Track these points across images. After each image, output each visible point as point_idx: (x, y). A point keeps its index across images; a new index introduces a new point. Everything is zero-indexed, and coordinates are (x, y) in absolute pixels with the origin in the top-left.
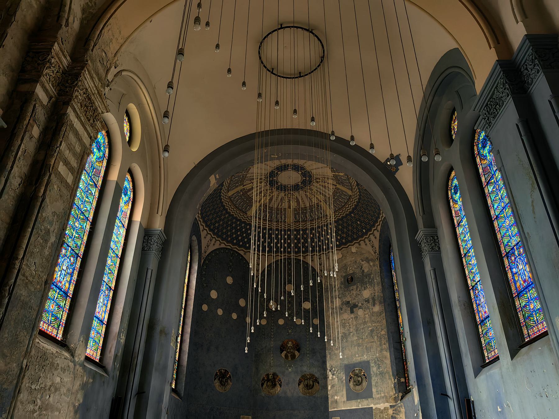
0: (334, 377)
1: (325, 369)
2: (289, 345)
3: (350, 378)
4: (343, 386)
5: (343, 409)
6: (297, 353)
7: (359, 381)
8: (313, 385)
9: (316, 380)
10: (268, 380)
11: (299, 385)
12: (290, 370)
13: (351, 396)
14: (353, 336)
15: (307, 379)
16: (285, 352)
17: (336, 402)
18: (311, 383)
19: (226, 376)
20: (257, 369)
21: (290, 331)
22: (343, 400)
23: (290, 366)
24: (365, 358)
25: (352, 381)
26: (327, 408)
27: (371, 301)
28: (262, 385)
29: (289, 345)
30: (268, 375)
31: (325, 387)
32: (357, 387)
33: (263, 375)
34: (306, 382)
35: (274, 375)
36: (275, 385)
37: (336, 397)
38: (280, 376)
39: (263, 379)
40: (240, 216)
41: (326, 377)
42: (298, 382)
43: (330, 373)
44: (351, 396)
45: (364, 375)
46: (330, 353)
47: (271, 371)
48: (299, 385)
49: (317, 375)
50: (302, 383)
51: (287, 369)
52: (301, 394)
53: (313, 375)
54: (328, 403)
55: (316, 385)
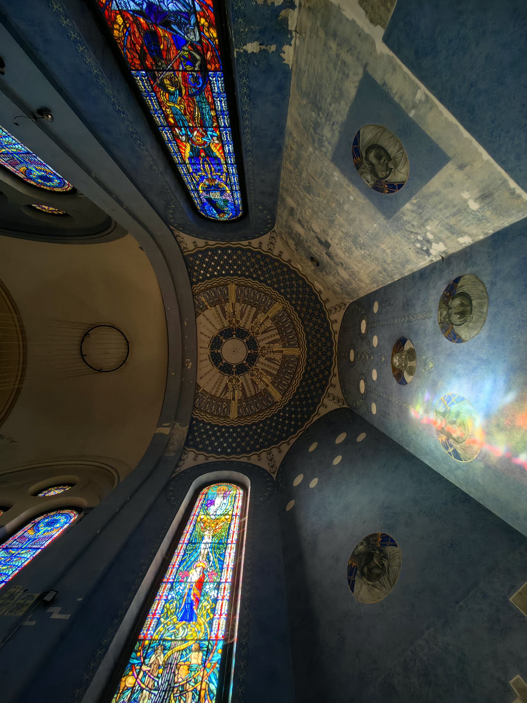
7: (378, 157)
12: (431, 365)
40: (275, 410)
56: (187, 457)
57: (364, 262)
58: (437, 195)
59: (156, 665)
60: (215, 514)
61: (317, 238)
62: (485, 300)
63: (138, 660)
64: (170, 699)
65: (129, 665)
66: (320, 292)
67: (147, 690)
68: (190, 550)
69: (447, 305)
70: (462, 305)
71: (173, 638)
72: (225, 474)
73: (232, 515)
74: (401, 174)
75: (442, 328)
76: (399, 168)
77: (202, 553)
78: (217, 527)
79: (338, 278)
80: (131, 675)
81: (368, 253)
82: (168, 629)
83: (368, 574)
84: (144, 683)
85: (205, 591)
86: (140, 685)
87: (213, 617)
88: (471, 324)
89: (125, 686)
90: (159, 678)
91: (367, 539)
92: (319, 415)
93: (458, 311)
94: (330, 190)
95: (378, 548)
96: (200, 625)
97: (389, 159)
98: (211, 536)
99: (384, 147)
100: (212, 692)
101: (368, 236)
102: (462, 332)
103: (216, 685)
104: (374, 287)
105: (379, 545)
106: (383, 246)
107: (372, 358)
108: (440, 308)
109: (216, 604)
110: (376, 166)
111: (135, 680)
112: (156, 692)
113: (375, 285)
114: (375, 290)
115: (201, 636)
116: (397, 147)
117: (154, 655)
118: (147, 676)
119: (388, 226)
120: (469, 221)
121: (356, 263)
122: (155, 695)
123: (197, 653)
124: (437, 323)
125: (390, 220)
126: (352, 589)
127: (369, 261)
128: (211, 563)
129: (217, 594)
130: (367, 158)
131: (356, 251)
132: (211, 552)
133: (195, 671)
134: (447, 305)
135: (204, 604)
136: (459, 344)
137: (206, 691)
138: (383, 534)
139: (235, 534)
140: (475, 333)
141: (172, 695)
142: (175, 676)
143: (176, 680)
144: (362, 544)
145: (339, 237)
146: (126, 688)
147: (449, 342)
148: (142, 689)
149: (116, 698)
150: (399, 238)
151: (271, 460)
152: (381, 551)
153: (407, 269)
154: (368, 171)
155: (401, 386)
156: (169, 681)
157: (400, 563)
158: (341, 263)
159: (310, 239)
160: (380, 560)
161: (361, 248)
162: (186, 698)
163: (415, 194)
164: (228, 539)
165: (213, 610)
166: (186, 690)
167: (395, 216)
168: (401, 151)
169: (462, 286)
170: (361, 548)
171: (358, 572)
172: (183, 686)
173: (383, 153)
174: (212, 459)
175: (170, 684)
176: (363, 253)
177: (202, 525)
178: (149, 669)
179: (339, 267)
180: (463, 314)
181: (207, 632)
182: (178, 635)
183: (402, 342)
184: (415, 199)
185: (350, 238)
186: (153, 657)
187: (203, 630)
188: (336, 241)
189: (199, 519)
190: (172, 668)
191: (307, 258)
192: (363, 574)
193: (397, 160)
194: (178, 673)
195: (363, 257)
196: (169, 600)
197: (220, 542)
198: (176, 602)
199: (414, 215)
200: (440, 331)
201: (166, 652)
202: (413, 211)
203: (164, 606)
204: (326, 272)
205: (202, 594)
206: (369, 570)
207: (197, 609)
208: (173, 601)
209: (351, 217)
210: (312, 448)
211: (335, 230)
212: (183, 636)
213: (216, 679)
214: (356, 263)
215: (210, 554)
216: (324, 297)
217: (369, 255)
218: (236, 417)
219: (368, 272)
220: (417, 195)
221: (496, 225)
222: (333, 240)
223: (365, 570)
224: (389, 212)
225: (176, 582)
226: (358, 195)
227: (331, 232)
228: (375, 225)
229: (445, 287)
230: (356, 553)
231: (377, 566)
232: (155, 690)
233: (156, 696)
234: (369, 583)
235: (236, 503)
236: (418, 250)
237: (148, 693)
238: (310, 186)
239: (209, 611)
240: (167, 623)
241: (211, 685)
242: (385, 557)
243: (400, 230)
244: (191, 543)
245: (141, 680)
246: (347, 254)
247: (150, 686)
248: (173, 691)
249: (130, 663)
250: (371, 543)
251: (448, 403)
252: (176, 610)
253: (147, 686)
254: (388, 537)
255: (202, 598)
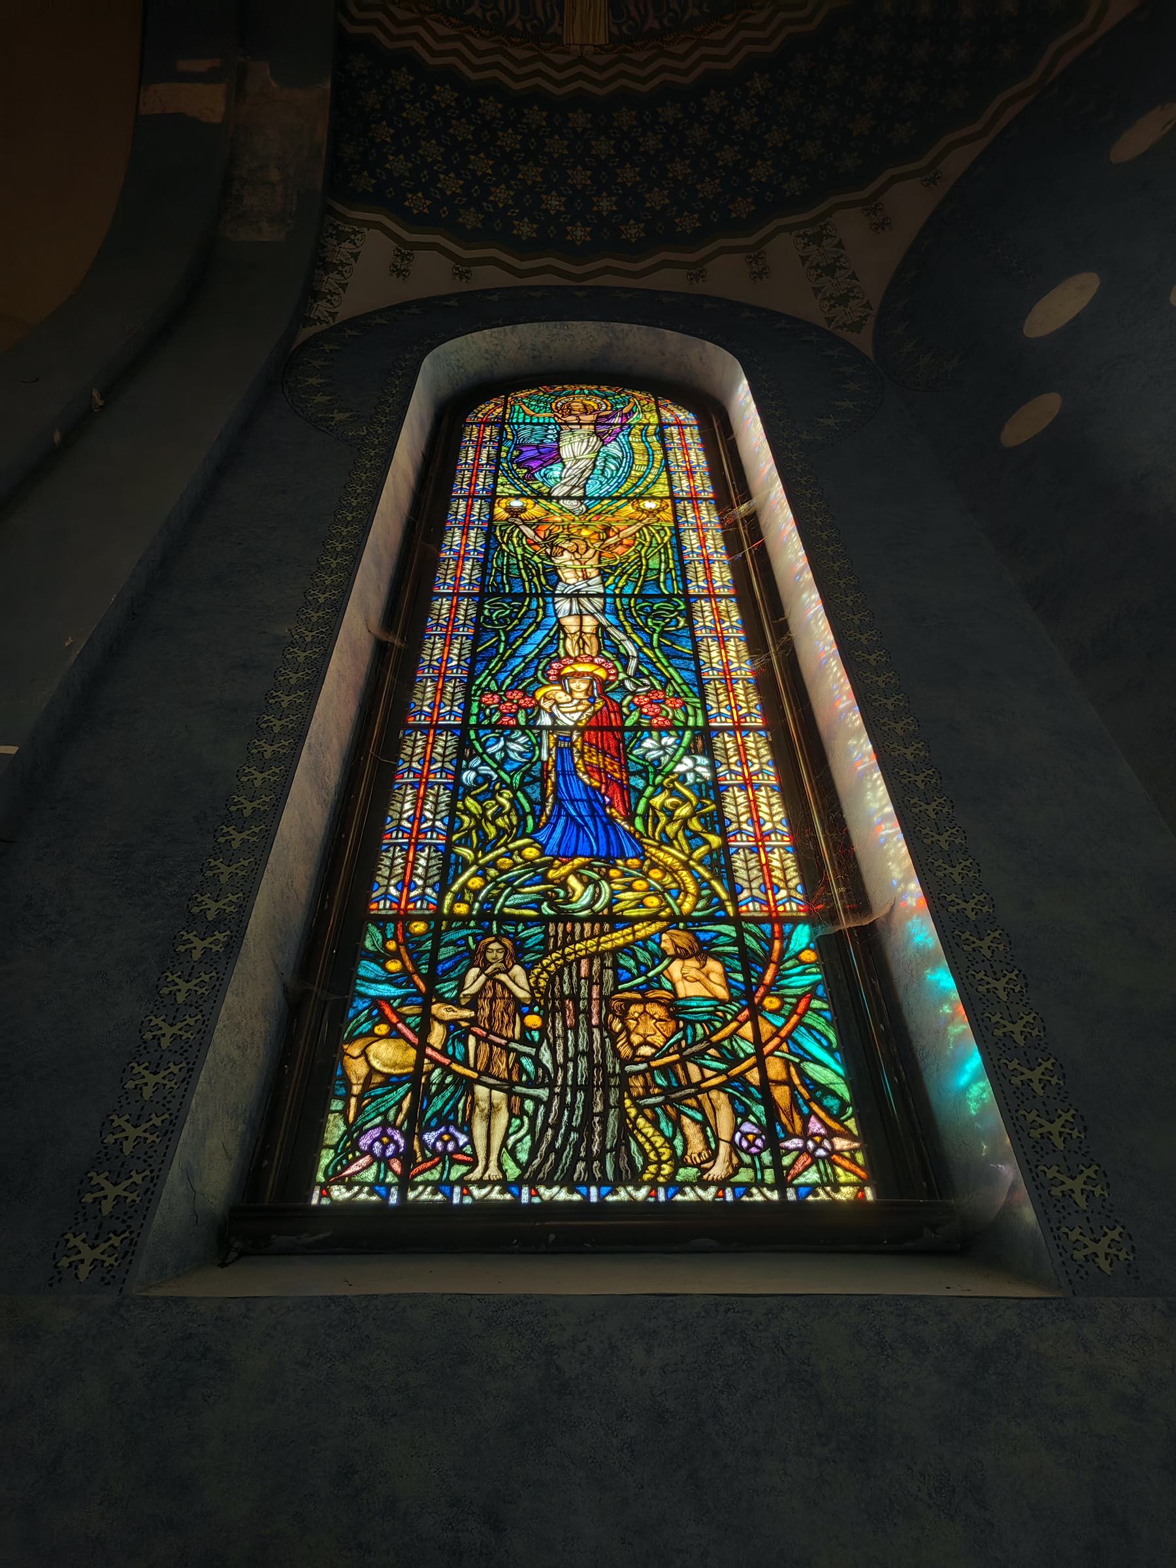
56: (355, 256)
59: (500, 1004)
60: (578, 493)
63: (398, 986)
64: (623, 1114)
65: (360, 1004)
67: (491, 1087)
68: (502, 620)
71: (546, 909)
72: (582, 337)
73: (673, 498)
77: (571, 624)
78: (611, 541)
80: (387, 1036)
82: (509, 883)
84: (465, 1063)
85: (643, 757)
86: (447, 1070)
87: (725, 847)
89: (372, 1070)
90: (537, 1046)
96: (667, 870)
98: (594, 573)
100: (828, 1091)
103: (840, 1071)
109: (719, 801)
111: (413, 1053)
112: (543, 1093)
115: (687, 907)
117: (474, 971)
118: (472, 1041)
122: (537, 1101)
123: (692, 963)
128: (633, 663)
129: (713, 767)
132: (621, 627)
133: (708, 1022)
135: (657, 801)
137: (793, 1087)
139: (715, 567)
141: (628, 1103)
142: (614, 1037)
143: (626, 1051)
146: (377, 1079)
148: (466, 1086)
149: (344, 1112)
151: (830, 270)
156: (589, 1054)
162: (700, 1109)
164: (685, 582)
165: (717, 822)
166: (690, 1085)
172: (665, 1070)
174: (488, 278)
175: (604, 1066)
177: (529, 532)
178: (467, 1013)
181: (715, 894)
182: (567, 900)
186: (474, 980)
187: (692, 888)
189: (500, 512)
190: (588, 1013)
194: (625, 1028)
196: (468, 791)
197: (651, 591)
198: (507, 793)
201: (528, 958)
203: (452, 806)
205: (633, 768)
207: (630, 820)
208: (493, 794)
212: (597, 907)
213: (829, 1049)
215: (618, 635)
218: (602, 40)
225: (478, 726)
232: (531, 1084)
233: (548, 1105)
235: (676, 456)
237: (498, 1096)
239: (695, 825)
240: (493, 864)
241: (811, 1068)
244: (498, 593)
245: (443, 1051)
247: (500, 1067)
248: (625, 1087)
249: (363, 996)
252: (522, 818)
253: (487, 1072)
255: (639, 782)
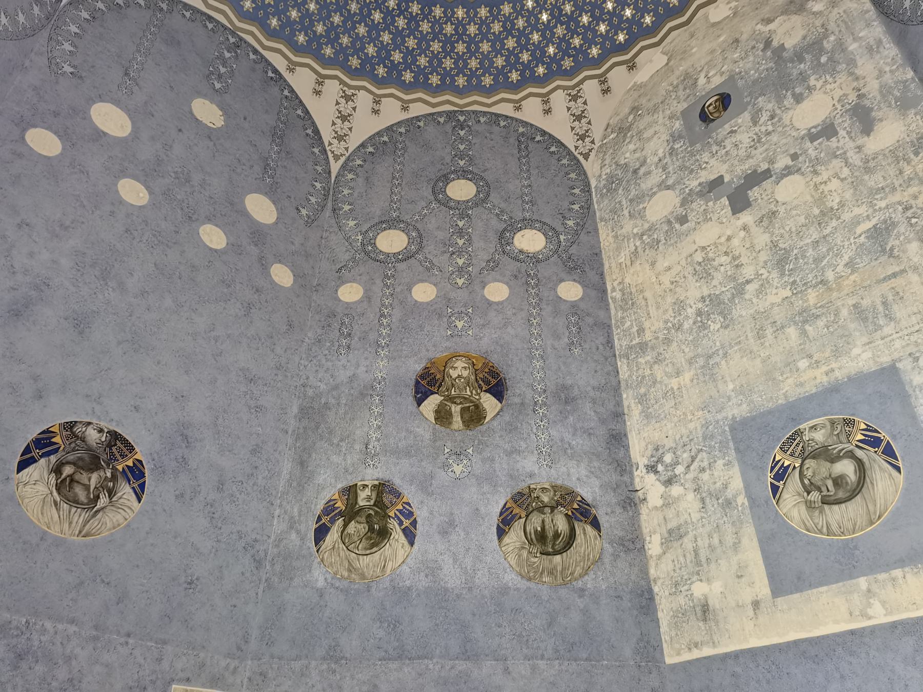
0: (676, 490)
1: (624, 467)
2: (454, 374)
3: (779, 477)
4: (737, 524)
5: (755, 642)
6: (489, 402)
7: (839, 481)
8: (572, 530)
9: (583, 513)
10: (351, 513)
11: (501, 533)
12: (458, 469)
13: (788, 576)
14: (760, 292)
15: (540, 510)
16: (434, 401)
17: (705, 610)
18: (562, 525)
19: (112, 459)
20: (302, 464)
21: (460, 324)
22: (747, 596)
23: (458, 455)
24: (861, 358)
25: (793, 484)
26: (649, 648)
27: (844, 124)
28: (321, 533)
29: (454, 374)
30: (351, 492)
31: (632, 543)
32: (835, 514)
33: (327, 488)
34: (535, 522)
35: (382, 488)
36: (384, 534)
37: (699, 589)
38: (410, 494)
39: (329, 509)
41: (631, 501)
42: (494, 520)
43: (652, 477)
44: (788, 576)
45: (874, 442)
46: (642, 399)
47: (371, 475)
48: (501, 533)
49: (586, 492)
50: (518, 525)
51: (445, 466)
52: (511, 578)
53: (571, 493)
54: (656, 621)
55: (584, 532)
57: (670, 300)
58: (735, 544)
61: (767, 174)
62: (560, 581)
66: (631, 66)
69: (558, 504)
70: (557, 535)
74: (792, 505)
75: (520, 494)
76: (803, 508)
79: (656, 177)
81: (686, 326)
83: (65, 479)
88: (525, 553)
91: (115, 437)
92: (291, 70)
93: (547, 527)
94: (844, 312)
95: (114, 468)
97: (826, 501)
99: (848, 503)
101: (716, 353)
102: (515, 537)
104: (614, 290)
105: (120, 468)
106: (687, 376)
107: (460, 282)
108: (555, 488)
110: (829, 464)
113: (618, 295)
114: (609, 288)
116: (834, 527)
119: (719, 417)
120: (680, 569)
121: (674, 272)
124: (529, 481)
125: (727, 428)
126: (23, 465)
127: (667, 316)
130: (851, 455)
131: (699, 296)
134: (558, 504)
136: (495, 531)
138: (140, 462)
140: (513, 563)
144: (101, 431)
145: (744, 260)
147: (499, 510)
150: (691, 426)
152: (114, 478)
153: (633, 405)
154: (830, 442)
155: (410, 392)
157: (119, 525)
158: (683, 220)
159: (774, 138)
160: (101, 486)
161: (699, 313)
163: (751, 508)
167: (731, 444)
168: (825, 530)
169: (585, 534)
170: (92, 436)
171: (53, 458)
173: (841, 494)
176: (689, 310)
179: (677, 201)
180: (541, 537)
183: (497, 385)
184: (743, 504)
185: (729, 295)
188: (736, 242)
191: (731, 79)
192: (57, 470)
193: (817, 513)
195: (680, 306)
199: (718, 485)
200: (515, 491)
202: (726, 486)
204: (680, 137)
206: (72, 479)
209: (769, 331)
210: (207, 112)
211: (763, 257)
214: (674, 272)
216: (618, 77)
217: (681, 325)
219: (648, 294)
220: (748, 511)
221: (663, 601)
222: (742, 234)
223: (68, 470)
224: (744, 435)
226: (801, 385)
227: (762, 239)
228: (731, 386)
229: (589, 498)
230: (78, 429)
231: (87, 488)
234: (55, 494)
236: (661, 451)
238: (884, 251)
242: (111, 493)
243: (705, 438)
246: (699, 257)
250: (114, 449)
251: (400, 511)
254: (143, 475)
